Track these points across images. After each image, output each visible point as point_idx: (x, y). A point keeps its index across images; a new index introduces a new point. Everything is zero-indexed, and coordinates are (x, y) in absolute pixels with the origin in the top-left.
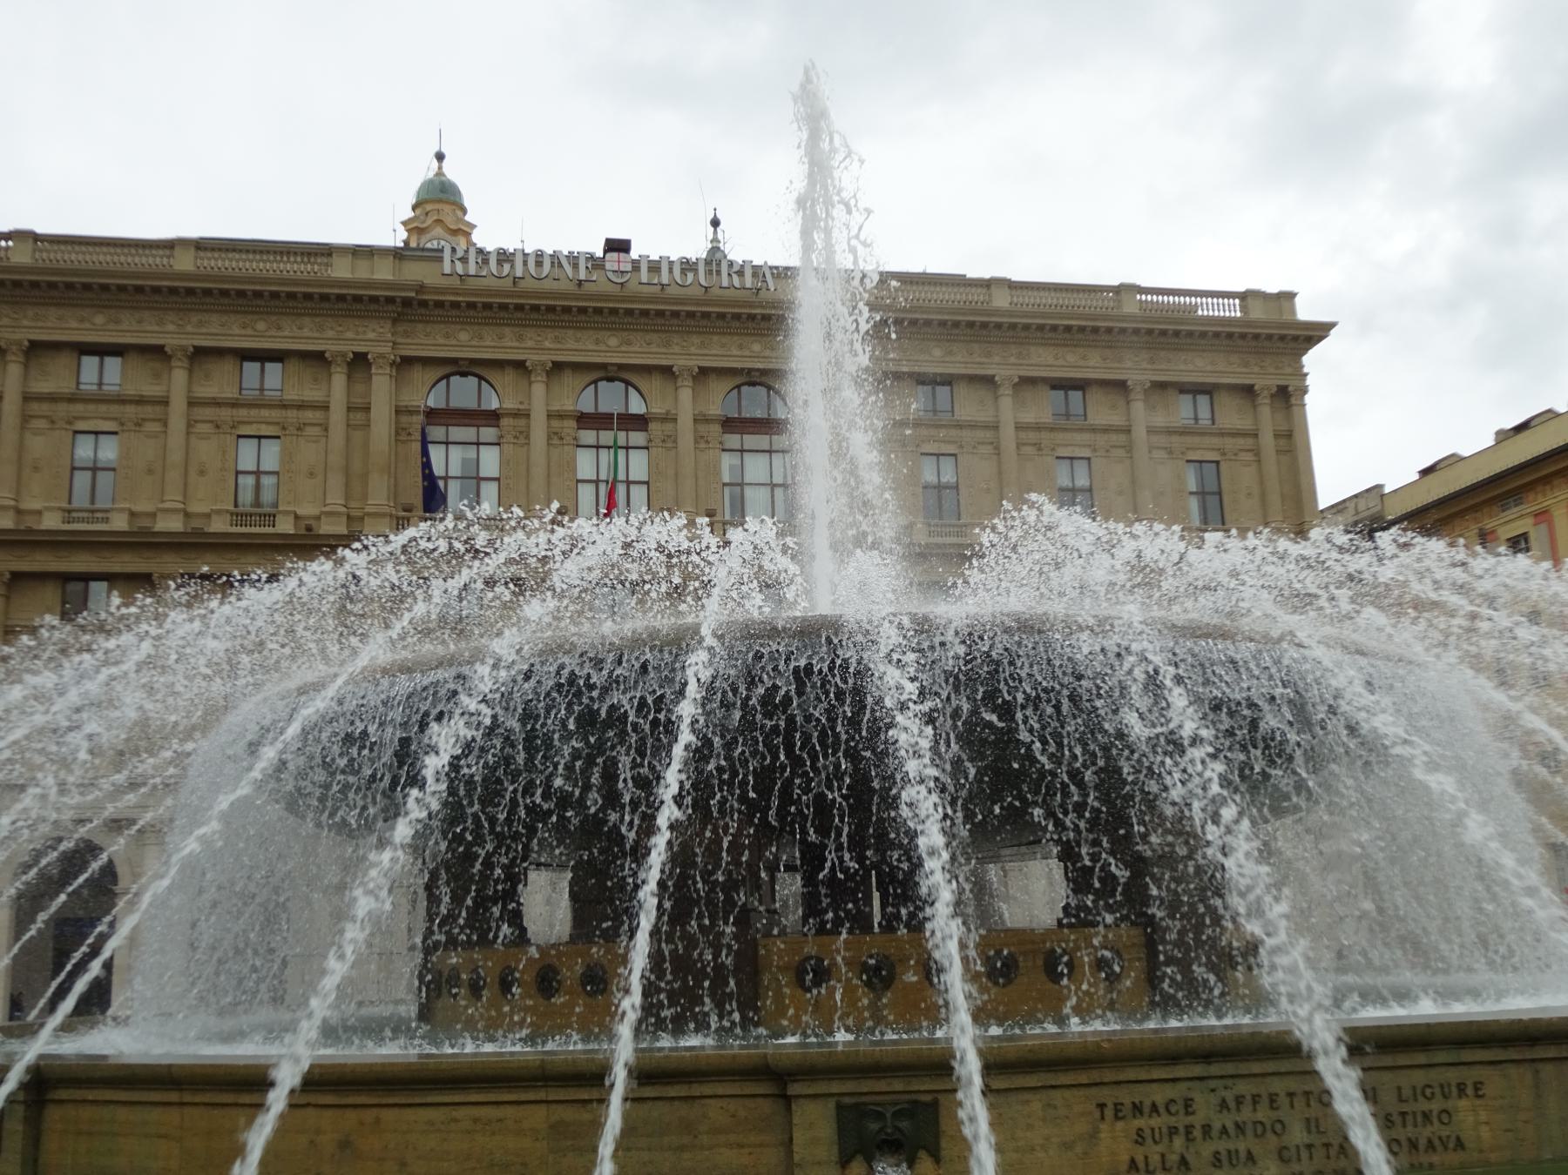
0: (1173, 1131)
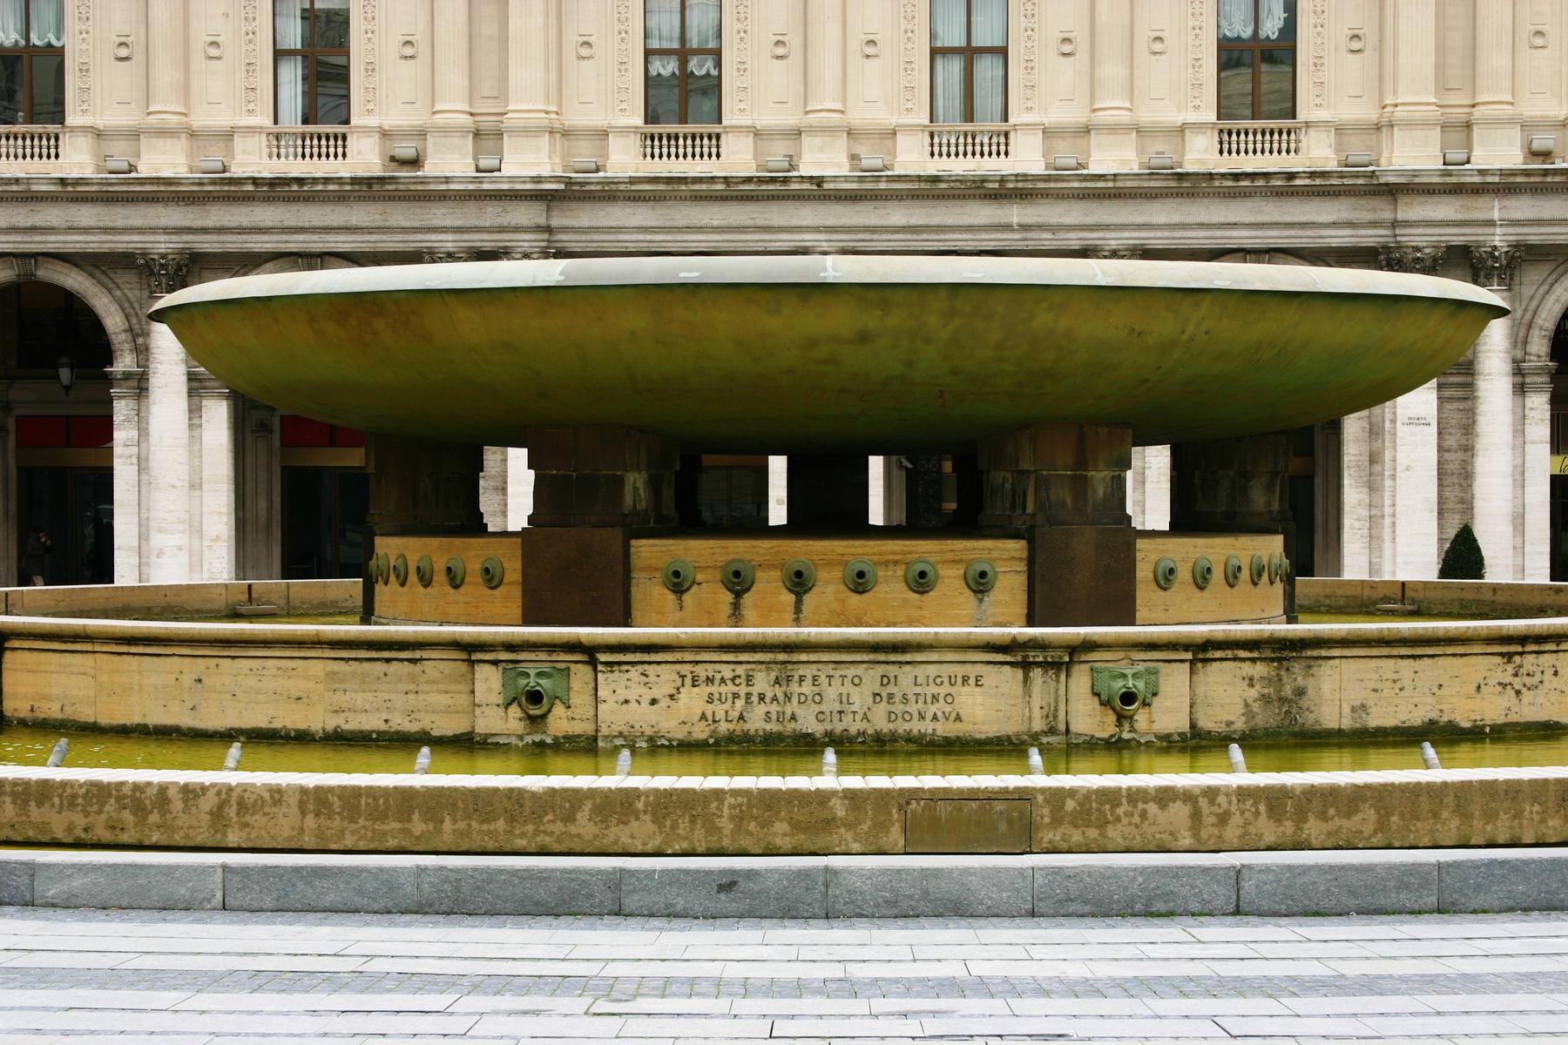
0: (736, 696)
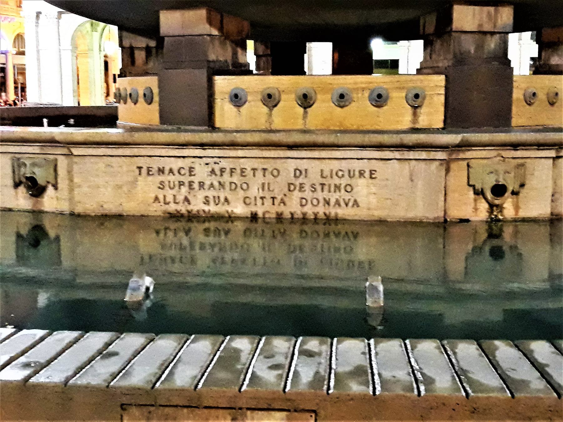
0: (181, 184)
